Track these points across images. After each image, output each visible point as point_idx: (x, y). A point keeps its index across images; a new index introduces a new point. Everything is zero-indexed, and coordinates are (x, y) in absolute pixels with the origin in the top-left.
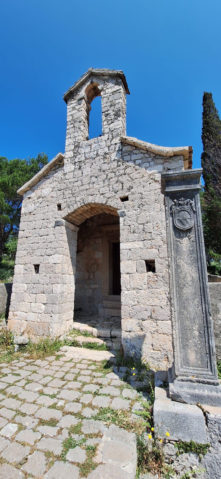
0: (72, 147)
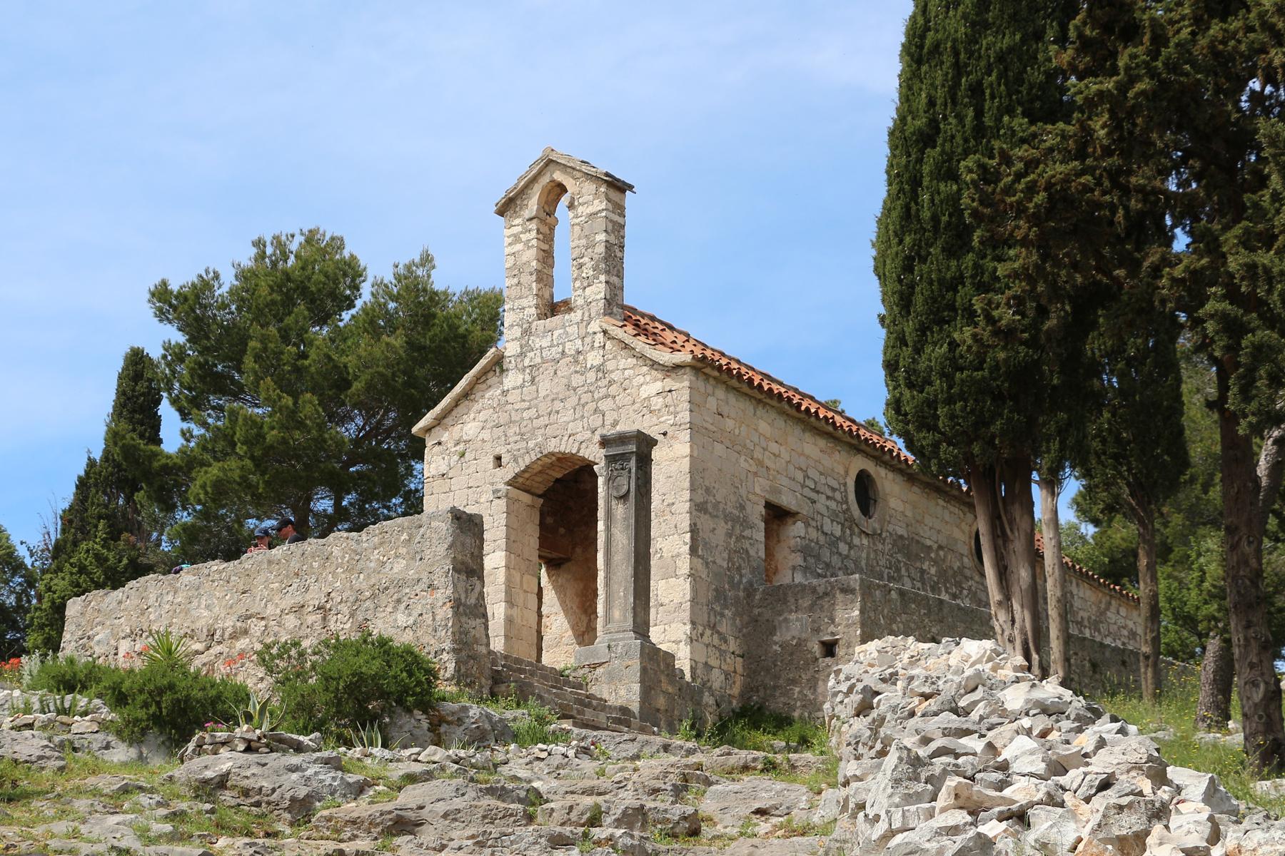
0: (517, 332)
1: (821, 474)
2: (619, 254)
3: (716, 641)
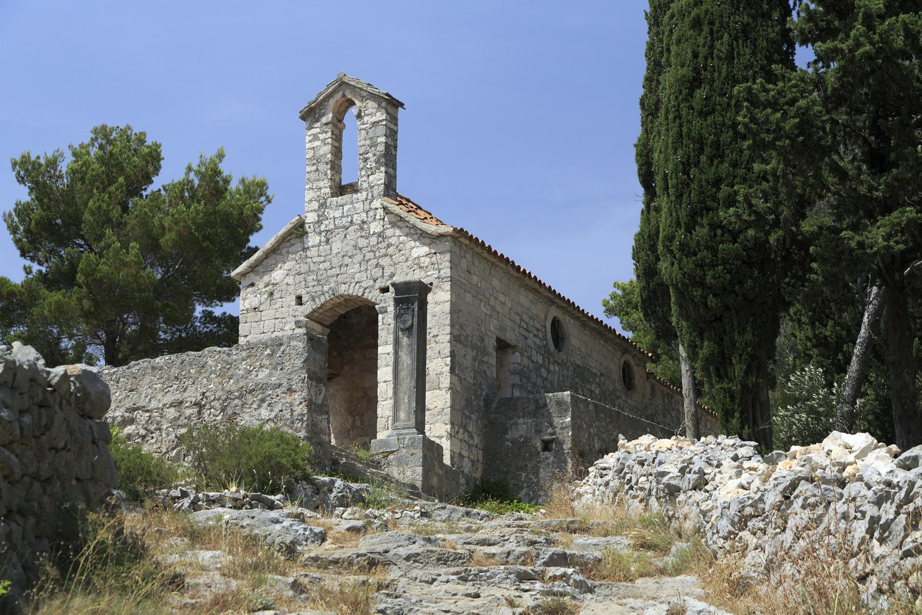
0: (315, 205)
1: (531, 318)
2: (394, 152)
3: (466, 438)
